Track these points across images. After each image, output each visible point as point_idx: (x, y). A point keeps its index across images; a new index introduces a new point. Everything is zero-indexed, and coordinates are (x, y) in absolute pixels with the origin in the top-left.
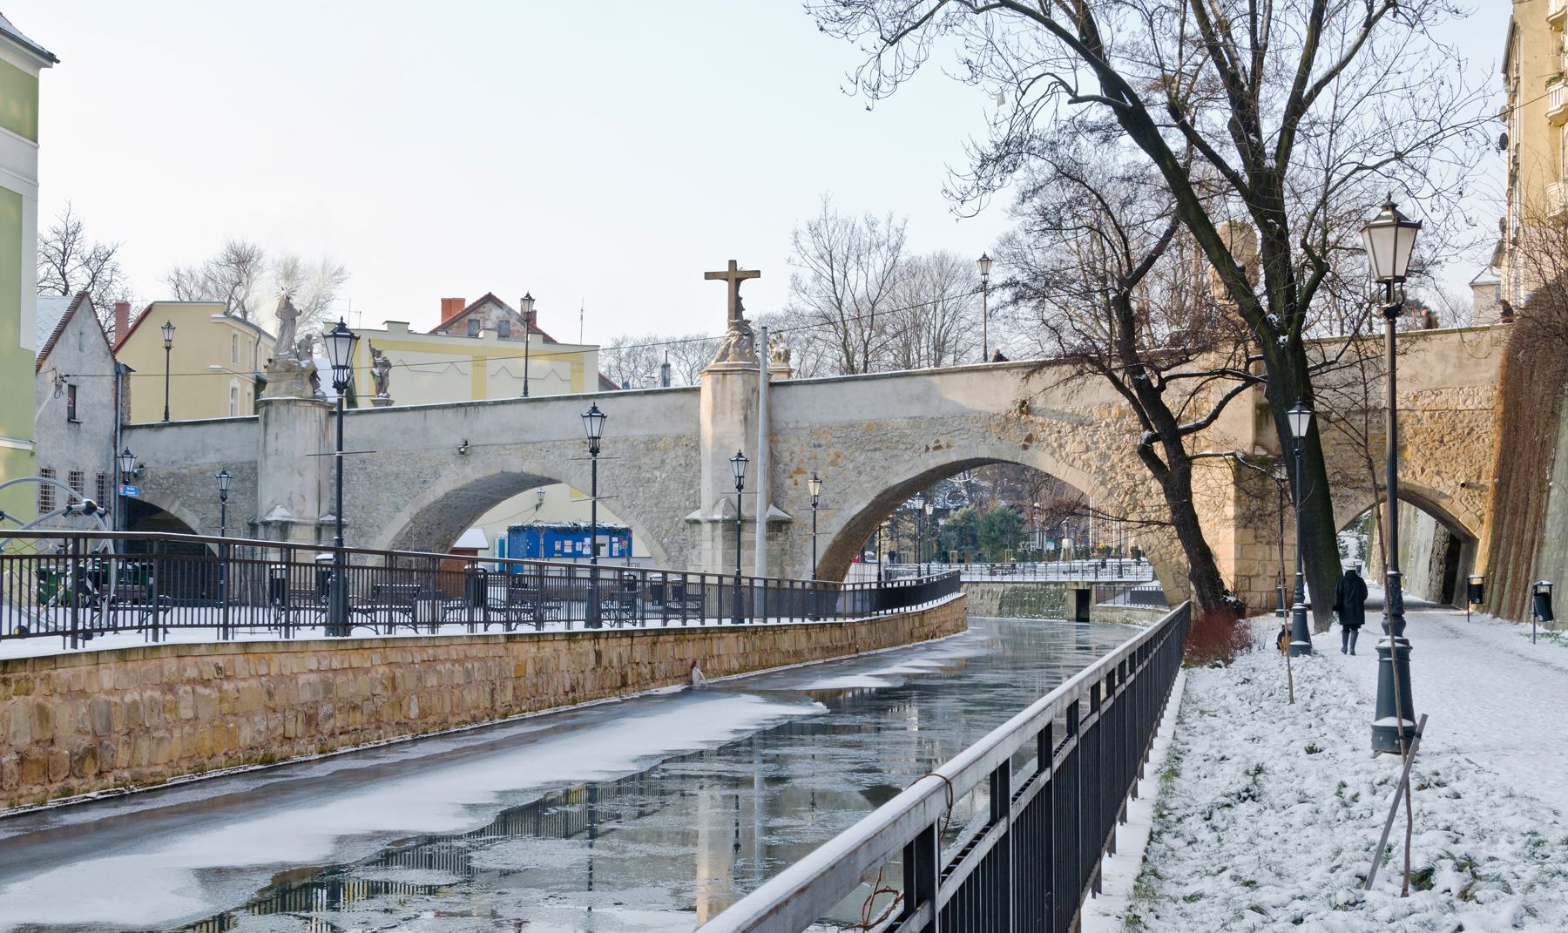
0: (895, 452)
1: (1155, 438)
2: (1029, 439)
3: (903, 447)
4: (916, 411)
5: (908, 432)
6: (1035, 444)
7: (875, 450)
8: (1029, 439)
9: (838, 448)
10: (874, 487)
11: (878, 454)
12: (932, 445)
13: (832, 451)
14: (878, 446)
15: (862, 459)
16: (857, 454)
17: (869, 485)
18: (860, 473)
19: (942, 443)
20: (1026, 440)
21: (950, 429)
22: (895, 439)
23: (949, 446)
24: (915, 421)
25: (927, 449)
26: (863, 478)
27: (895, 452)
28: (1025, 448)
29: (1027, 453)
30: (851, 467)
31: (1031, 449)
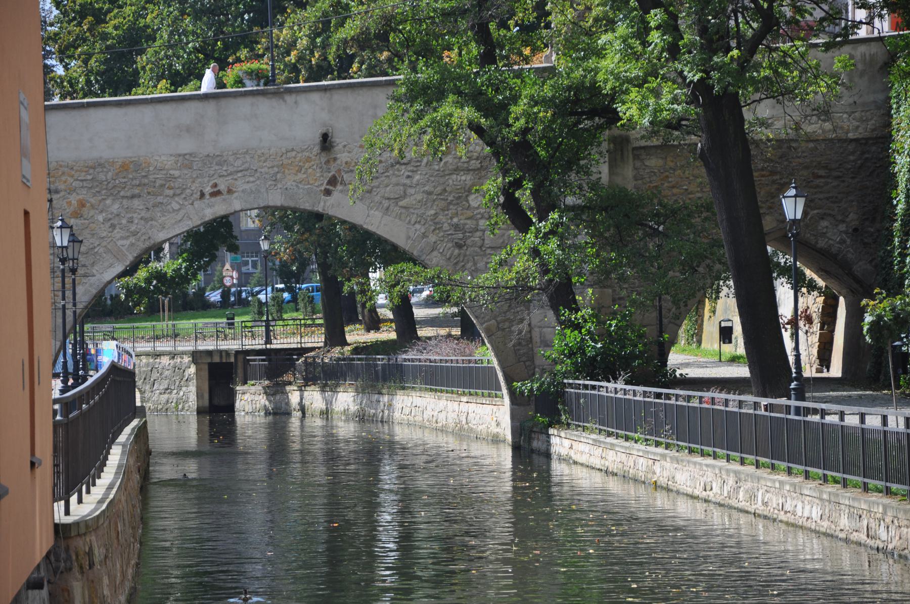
0: (160, 199)
1: (517, 184)
2: (333, 181)
3: (171, 192)
4: (186, 145)
5: (176, 173)
6: (339, 187)
7: (133, 197)
8: (333, 181)
9: (83, 195)
10: (132, 245)
11: (136, 202)
12: (208, 190)
13: (74, 199)
14: (137, 191)
15: (115, 208)
16: (108, 202)
17: (127, 242)
18: (113, 226)
19: (222, 187)
20: (329, 183)
21: (231, 169)
22: (158, 183)
23: (230, 191)
24: (186, 160)
25: (202, 195)
26: (118, 233)
27: (160, 199)
28: (328, 193)
29: (330, 200)
30: (100, 218)
31: (336, 195)
